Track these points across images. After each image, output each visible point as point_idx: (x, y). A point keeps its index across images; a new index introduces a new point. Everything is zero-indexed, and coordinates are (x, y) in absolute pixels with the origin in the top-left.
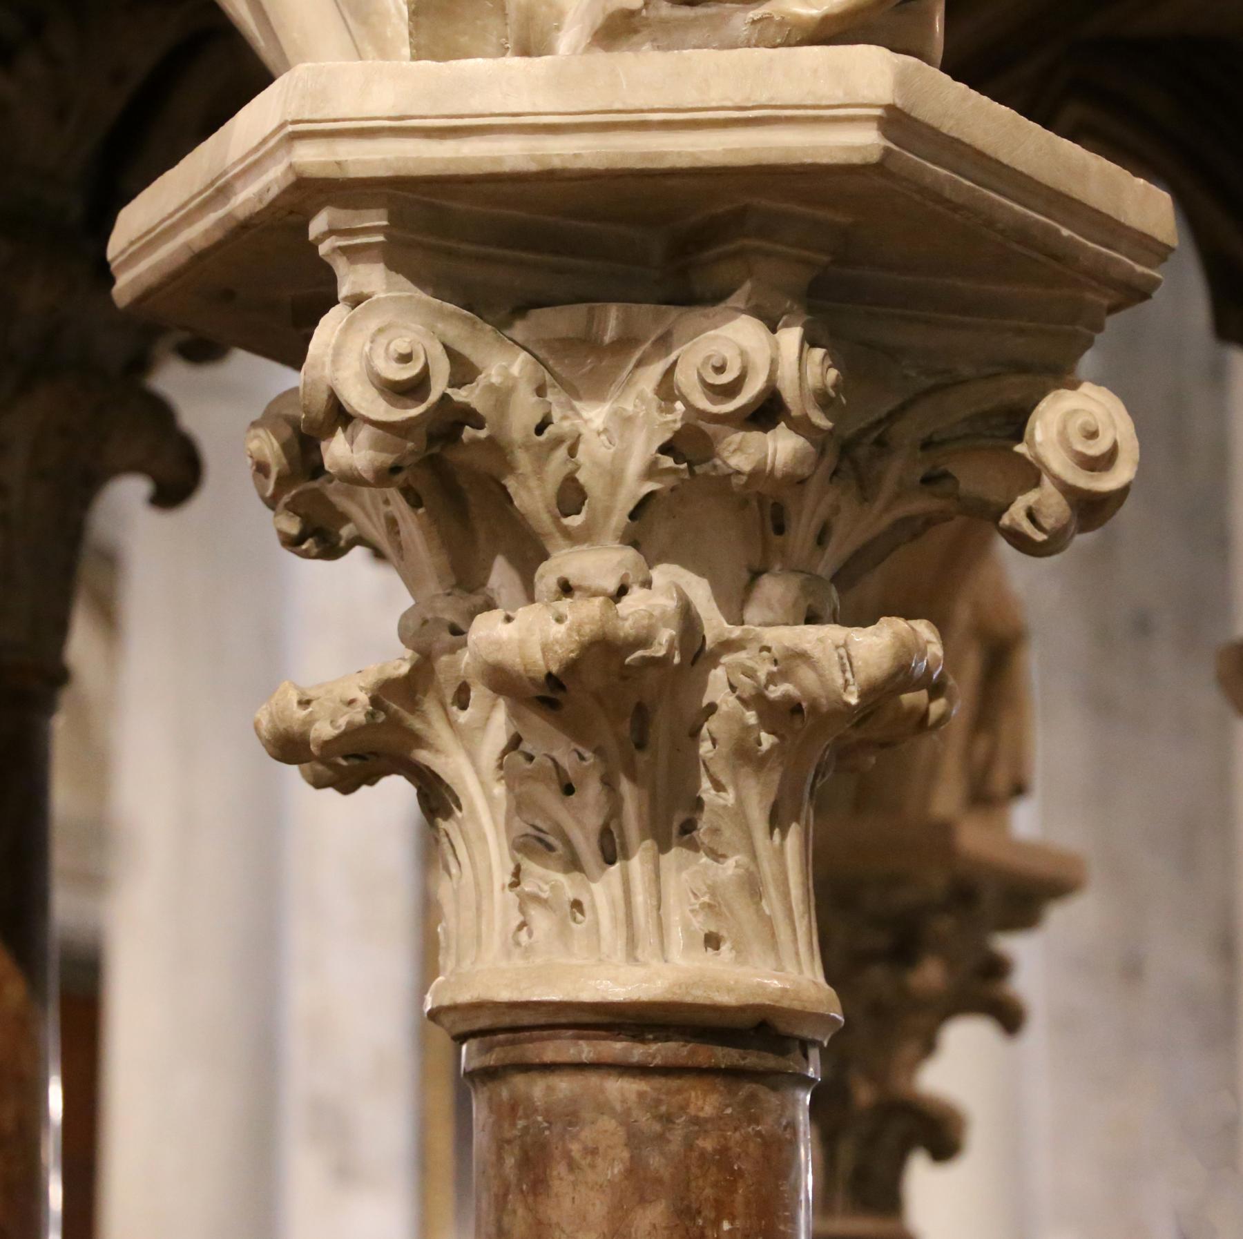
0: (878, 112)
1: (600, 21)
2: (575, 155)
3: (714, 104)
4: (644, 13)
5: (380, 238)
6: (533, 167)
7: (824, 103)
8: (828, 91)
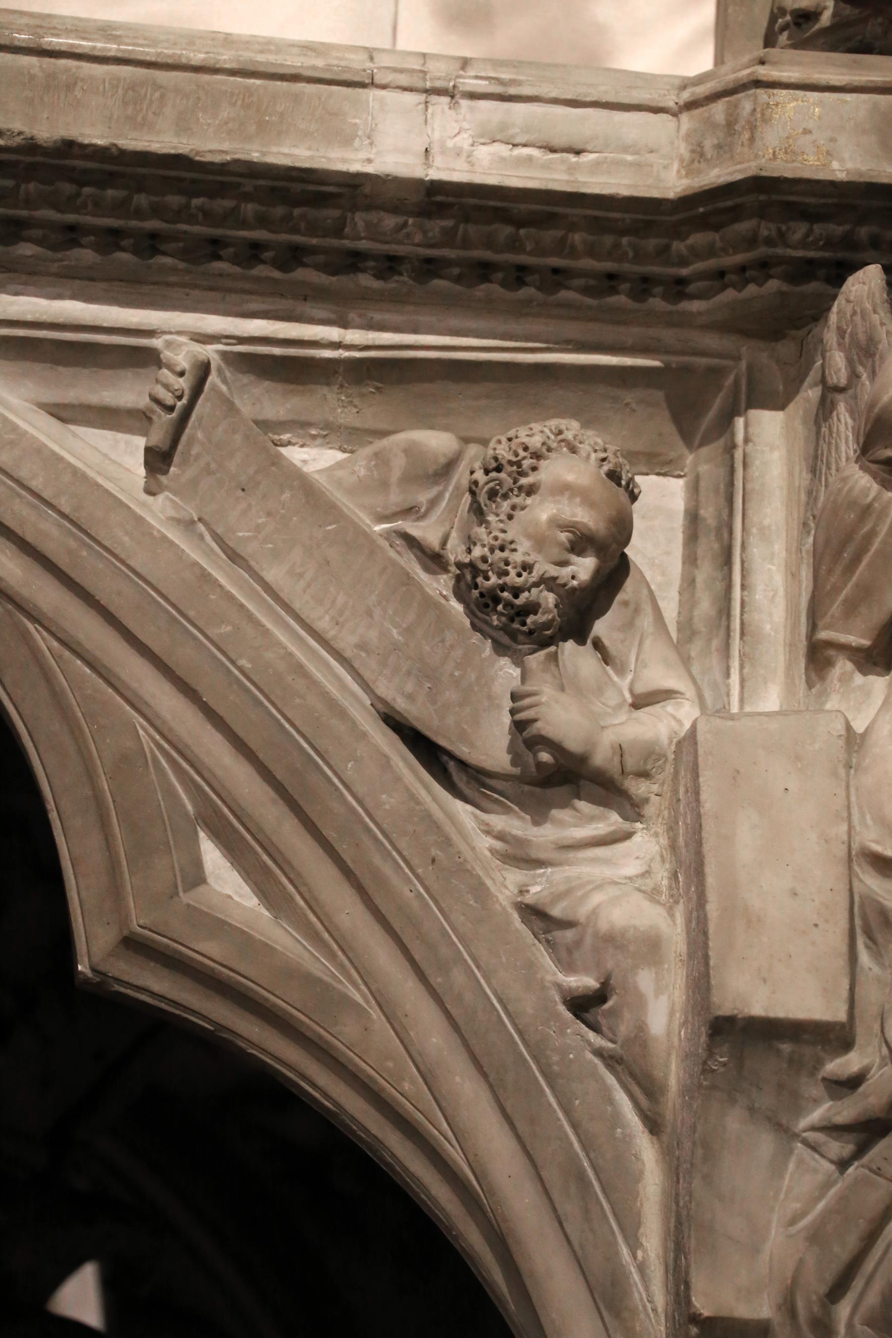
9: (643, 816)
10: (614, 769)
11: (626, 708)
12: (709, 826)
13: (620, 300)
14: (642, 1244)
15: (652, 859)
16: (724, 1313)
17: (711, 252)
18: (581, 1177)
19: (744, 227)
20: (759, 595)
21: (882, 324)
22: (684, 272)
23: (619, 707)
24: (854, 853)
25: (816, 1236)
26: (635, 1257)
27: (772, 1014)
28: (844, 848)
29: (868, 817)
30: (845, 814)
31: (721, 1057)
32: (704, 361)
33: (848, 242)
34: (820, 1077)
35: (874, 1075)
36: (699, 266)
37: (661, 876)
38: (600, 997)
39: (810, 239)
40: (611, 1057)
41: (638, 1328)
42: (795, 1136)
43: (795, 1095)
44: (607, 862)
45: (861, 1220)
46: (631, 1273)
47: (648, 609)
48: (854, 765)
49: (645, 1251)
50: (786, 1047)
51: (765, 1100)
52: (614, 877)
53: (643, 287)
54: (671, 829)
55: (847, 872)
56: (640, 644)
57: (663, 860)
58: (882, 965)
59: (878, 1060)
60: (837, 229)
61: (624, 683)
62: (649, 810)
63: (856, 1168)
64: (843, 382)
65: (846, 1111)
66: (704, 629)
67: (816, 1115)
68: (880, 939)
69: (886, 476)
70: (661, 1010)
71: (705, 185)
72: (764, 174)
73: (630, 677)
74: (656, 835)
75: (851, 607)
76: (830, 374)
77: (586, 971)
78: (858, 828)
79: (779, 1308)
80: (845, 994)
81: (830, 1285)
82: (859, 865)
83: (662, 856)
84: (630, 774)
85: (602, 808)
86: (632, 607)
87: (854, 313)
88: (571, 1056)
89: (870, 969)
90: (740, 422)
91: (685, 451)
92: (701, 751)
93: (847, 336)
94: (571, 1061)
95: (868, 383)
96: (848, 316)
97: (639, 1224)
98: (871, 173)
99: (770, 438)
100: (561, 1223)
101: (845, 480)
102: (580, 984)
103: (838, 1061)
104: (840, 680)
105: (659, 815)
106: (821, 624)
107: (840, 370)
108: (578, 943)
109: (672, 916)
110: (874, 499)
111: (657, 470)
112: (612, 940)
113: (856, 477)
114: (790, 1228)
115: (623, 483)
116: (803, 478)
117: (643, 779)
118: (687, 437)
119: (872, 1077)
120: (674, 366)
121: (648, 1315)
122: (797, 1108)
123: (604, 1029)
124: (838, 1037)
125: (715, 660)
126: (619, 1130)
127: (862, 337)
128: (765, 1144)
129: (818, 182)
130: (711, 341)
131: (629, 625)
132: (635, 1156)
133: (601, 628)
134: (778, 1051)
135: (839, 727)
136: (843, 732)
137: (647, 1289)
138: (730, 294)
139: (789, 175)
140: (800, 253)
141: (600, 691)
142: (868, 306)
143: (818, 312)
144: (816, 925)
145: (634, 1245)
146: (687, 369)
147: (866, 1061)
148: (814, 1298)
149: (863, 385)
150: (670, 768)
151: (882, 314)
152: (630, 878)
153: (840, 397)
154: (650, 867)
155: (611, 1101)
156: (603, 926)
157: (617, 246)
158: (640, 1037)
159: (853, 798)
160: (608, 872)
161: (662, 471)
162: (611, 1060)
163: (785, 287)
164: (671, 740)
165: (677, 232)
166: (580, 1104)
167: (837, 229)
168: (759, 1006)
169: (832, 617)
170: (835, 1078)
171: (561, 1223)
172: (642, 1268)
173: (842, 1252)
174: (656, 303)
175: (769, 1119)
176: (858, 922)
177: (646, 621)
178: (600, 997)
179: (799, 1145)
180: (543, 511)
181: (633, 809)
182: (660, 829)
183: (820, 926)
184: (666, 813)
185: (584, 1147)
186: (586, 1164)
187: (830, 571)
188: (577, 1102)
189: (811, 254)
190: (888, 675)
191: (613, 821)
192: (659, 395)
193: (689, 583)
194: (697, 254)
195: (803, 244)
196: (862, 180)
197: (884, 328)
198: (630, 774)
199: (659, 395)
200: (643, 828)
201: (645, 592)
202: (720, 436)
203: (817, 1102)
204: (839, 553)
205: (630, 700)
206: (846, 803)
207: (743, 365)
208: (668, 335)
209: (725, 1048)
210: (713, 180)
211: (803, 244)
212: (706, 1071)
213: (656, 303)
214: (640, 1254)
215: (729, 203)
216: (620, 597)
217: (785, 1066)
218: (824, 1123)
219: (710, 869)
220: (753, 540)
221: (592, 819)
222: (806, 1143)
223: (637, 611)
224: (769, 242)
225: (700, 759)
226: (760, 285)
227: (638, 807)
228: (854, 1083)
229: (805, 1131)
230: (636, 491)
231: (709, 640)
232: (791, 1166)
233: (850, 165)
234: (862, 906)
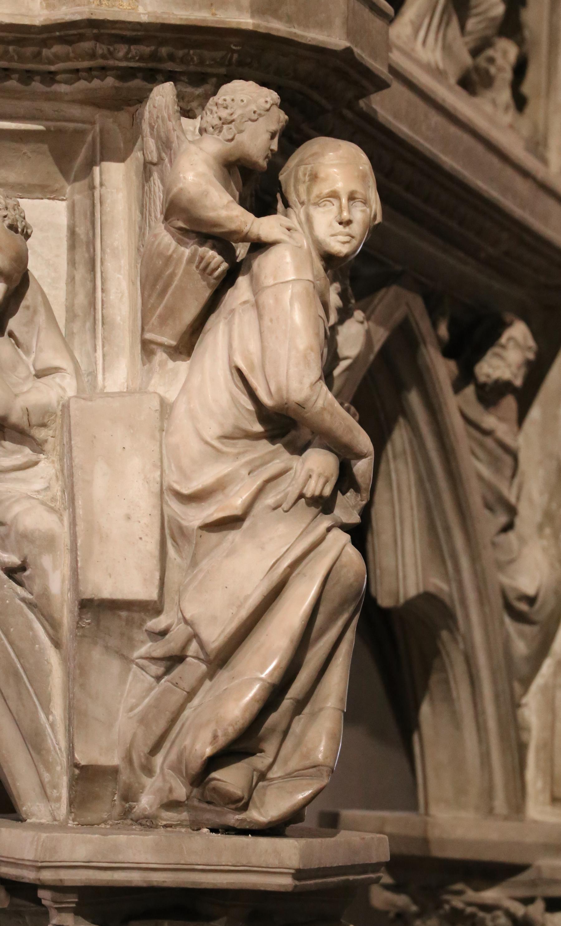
0: (292, 871)
1: (165, 800)
2: (164, 882)
3: (224, 863)
4: (186, 802)
5: (74, 905)
6: (145, 885)
7: (270, 866)
8: (273, 861)
9: (44, 451)
10: (24, 423)
11: (32, 378)
12: (78, 474)
14: (52, 712)
15: (51, 479)
16: (93, 763)
17: (67, 58)
18: (16, 674)
19: (86, 45)
20: (113, 296)
21: (174, 130)
22: (53, 68)
23: (27, 378)
24: (164, 488)
25: (143, 720)
26: (48, 719)
27: (114, 597)
28: (159, 485)
29: (173, 465)
30: (159, 464)
31: (87, 620)
33: (154, 57)
34: (144, 629)
35: (174, 629)
37: (57, 489)
38: (23, 568)
39: (130, 56)
40: (30, 604)
41: (50, 760)
42: (133, 661)
43: (131, 639)
44: (24, 481)
45: (167, 712)
46: (46, 727)
47: (42, 310)
48: (165, 429)
49: (54, 716)
50: (124, 614)
51: (113, 642)
52: (27, 493)
53: (27, 76)
54: (61, 460)
55: (160, 503)
56: (39, 332)
57: (57, 479)
58: (181, 557)
59: (176, 621)
60: (146, 50)
61: (30, 361)
62: (48, 447)
63: (165, 682)
64: (155, 160)
65: (160, 649)
66: (81, 314)
67: (143, 650)
68: (180, 543)
69: (180, 236)
70: (55, 580)
71: (59, 19)
72: (94, 17)
73: (33, 356)
74: (53, 462)
75: (163, 320)
76: (147, 154)
77: (13, 552)
78: (167, 472)
79: (123, 759)
80: (157, 582)
81: (150, 748)
82: (168, 495)
83: (57, 476)
84: (34, 426)
85: (19, 446)
86: (31, 309)
87: (158, 117)
88: (7, 602)
89: (175, 559)
90: (97, 170)
91: (66, 184)
92: (72, 422)
93: (155, 130)
94: (8, 604)
95: (169, 165)
96: (155, 117)
97: (50, 701)
98: (165, 16)
99: (116, 179)
100: (5, 700)
101: (155, 236)
102: (10, 560)
103: (154, 621)
104: (159, 365)
105: (54, 450)
106: (146, 328)
107: (152, 151)
108: (7, 536)
109: (61, 520)
110: (174, 252)
111: (48, 196)
112: (25, 537)
113: (162, 235)
114: (130, 713)
115: (20, 230)
116: (137, 215)
117: (43, 428)
118: (65, 173)
119: (173, 630)
120: (52, 129)
121: (56, 751)
122: (133, 647)
123: (26, 585)
124: (154, 608)
125: (88, 336)
126: (37, 646)
127: (162, 134)
128: (115, 666)
129: (130, 23)
130: (76, 111)
131: (30, 322)
132: (47, 660)
133: (13, 324)
134: (119, 616)
135: (156, 404)
136: (158, 407)
137: (55, 737)
138: (82, 84)
139: (110, 18)
140: (124, 64)
141: (14, 368)
142: (166, 115)
143: (141, 98)
144: (141, 538)
145: (48, 712)
146: (60, 131)
147: (169, 622)
148: (142, 754)
149: (166, 166)
150: (59, 421)
151: (174, 123)
152: (38, 492)
153: (154, 168)
154: (49, 483)
155: (31, 628)
156: (21, 528)
157: (6, 52)
158: (45, 594)
159: (164, 452)
160: (23, 488)
161: (52, 197)
162: (31, 605)
163: (117, 84)
164: (58, 402)
165: (45, 43)
166: (13, 630)
167: (146, 50)
168: (108, 591)
169: (153, 324)
170: (152, 631)
171: (5, 700)
172: (52, 725)
173: (158, 729)
174: (37, 85)
175: (117, 652)
176: (167, 531)
177: (41, 318)
178: (23, 568)
179: (134, 666)
181: (38, 446)
182: (55, 458)
183: (143, 539)
184: (58, 448)
185: (17, 656)
186: (19, 666)
187: (150, 296)
188: (12, 630)
189: (132, 64)
190: (189, 360)
191: (25, 454)
192: (45, 147)
193: (71, 280)
194: (58, 58)
195: (126, 58)
196: (158, 21)
197: (175, 132)
198: (34, 426)
199: (45, 147)
200: (45, 458)
201: (40, 298)
202: (84, 178)
203: (143, 642)
204: (154, 286)
205: (34, 373)
206: (159, 457)
207: (97, 128)
208: (47, 107)
209: (89, 615)
210: (63, 16)
211: (126, 58)
212: (78, 627)
213: (37, 85)
214: (51, 718)
215: (74, 32)
216: (23, 303)
217: (124, 623)
218: (148, 656)
219: (79, 503)
220: (107, 257)
221: (13, 452)
222: (137, 664)
223: (35, 312)
224: (103, 57)
225: (72, 428)
226: (102, 80)
227: (41, 445)
228: (163, 633)
229: (137, 659)
230: (29, 231)
231: (85, 322)
232: (130, 678)
233: (150, 9)
234: (169, 521)
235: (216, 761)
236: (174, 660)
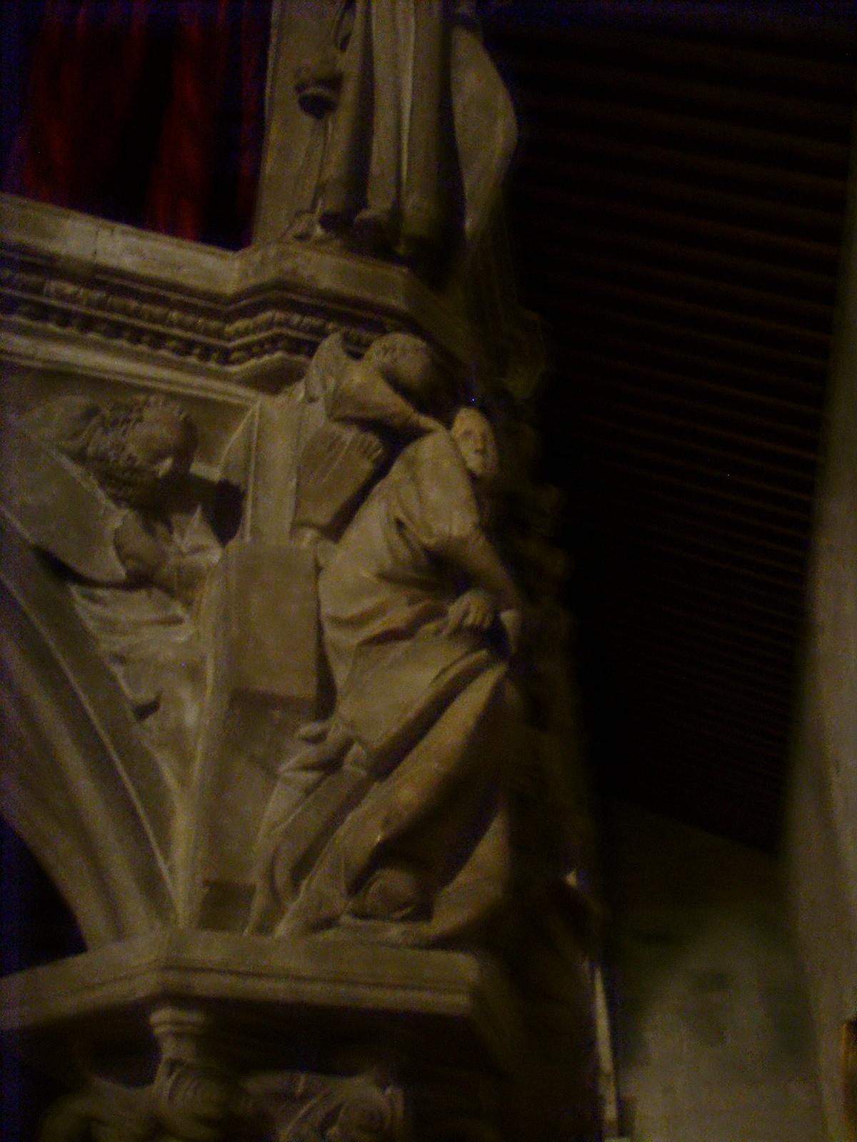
13: (193, 360)
17: (246, 332)
32: (235, 401)
36: (239, 342)
53: (206, 353)
163: (286, 356)
174: (212, 365)
180: (142, 431)
194: (240, 334)
235: (385, 855)
236: (330, 765)
